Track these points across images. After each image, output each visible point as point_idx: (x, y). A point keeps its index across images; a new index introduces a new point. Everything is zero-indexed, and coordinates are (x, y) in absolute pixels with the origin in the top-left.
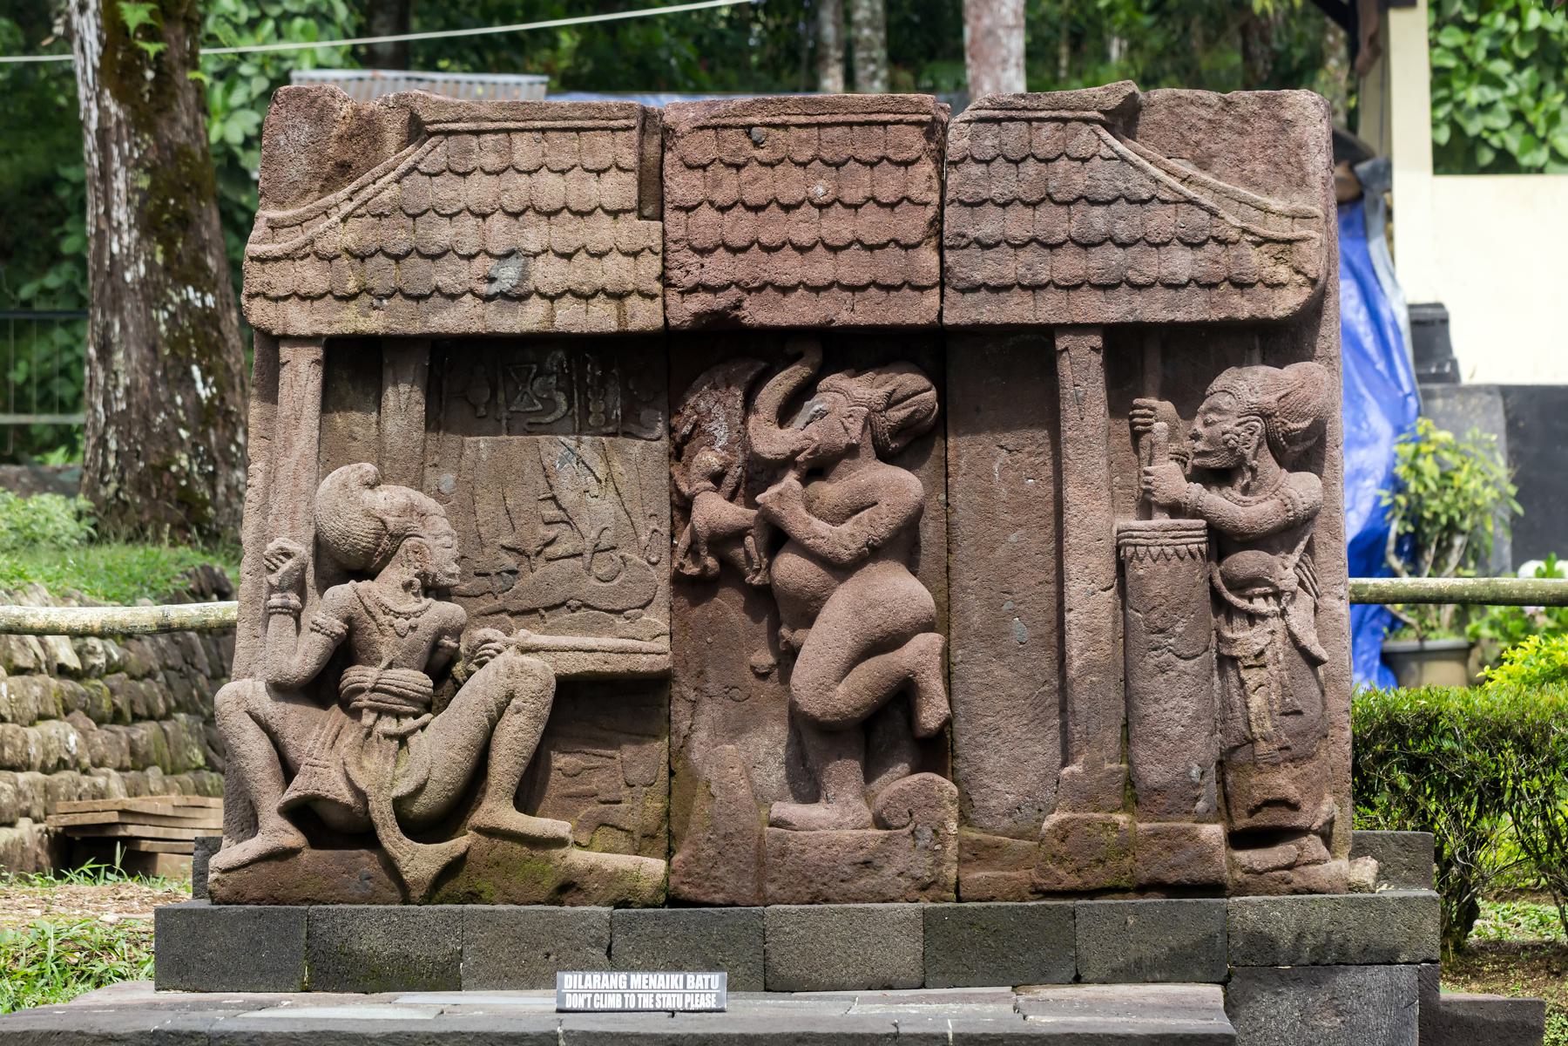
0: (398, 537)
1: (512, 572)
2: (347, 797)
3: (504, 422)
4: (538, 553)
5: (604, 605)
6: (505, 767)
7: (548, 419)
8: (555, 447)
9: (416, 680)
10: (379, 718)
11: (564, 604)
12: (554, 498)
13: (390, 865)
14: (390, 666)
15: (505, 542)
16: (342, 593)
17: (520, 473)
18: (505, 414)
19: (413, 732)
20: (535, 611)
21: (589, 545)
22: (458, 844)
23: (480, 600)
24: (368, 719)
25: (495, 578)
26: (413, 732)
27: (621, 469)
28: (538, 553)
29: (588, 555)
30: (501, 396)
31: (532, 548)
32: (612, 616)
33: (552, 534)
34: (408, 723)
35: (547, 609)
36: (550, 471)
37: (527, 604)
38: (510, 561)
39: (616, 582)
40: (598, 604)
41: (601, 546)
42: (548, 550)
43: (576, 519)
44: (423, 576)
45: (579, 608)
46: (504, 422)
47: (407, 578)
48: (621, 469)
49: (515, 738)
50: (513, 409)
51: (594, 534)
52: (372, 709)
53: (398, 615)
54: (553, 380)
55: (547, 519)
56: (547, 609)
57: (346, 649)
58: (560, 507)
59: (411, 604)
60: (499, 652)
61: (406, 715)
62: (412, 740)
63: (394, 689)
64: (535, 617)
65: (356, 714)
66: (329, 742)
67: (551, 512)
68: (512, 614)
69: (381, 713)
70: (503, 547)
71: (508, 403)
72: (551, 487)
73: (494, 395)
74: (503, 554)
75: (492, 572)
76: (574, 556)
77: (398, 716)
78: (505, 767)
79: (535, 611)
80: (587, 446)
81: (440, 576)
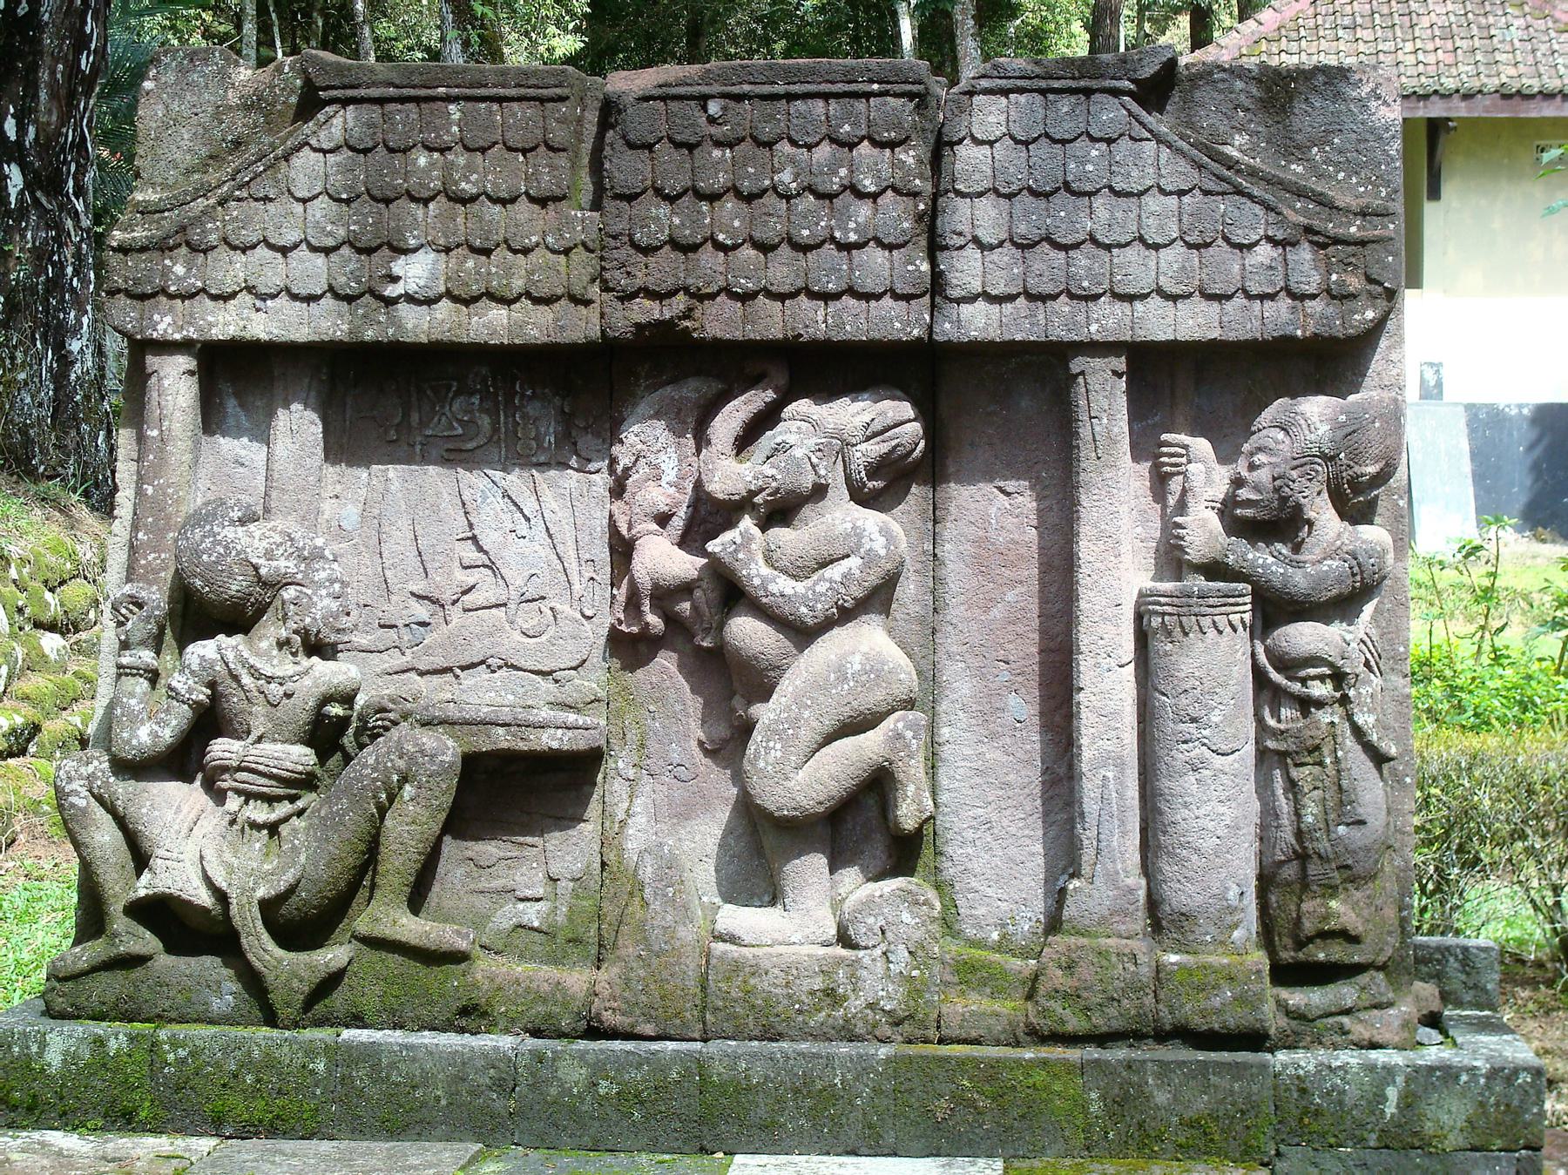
0: (274, 585)
1: (423, 624)
2: (204, 898)
3: (418, 448)
4: (454, 602)
5: (529, 665)
6: (398, 861)
7: (470, 446)
8: (475, 482)
9: (300, 756)
10: (246, 802)
11: (483, 662)
12: (474, 539)
13: (253, 981)
14: (259, 740)
15: (415, 589)
16: (204, 650)
17: (435, 509)
18: (419, 439)
19: (286, 819)
20: (448, 670)
21: (514, 595)
22: (333, 955)
23: (384, 656)
24: (233, 803)
25: (403, 631)
26: (286, 819)
27: (554, 506)
28: (454, 602)
29: (512, 606)
30: (415, 417)
31: (447, 597)
32: (538, 678)
33: (471, 581)
34: (284, 809)
35: (463, 668)
36: (469, 507)
37: (440, 662)
38: (422, 611)
39: (544, 638)
40: (522, 663)
41: (528, 596)
42: (465, 598)
43: (498, 564)
44: (304, 633)
45: (500, 667)
46: (418, 448)
47: (284, 633)
48: (554, 506)
49: (408, 828)
50: (430, 432)
51: (520, 582)
52: (238, 792)
53: (269, 680)
54: (476, 400)
55: (466, 562)
56: (463, 668)
57: (210, 720)
58: (480, 549)
59: (283, 666)
60: (395, 723)
61: (279, 799)
62: (284, 830)
63: (261, 768)
64: (449, 677)
65: (219, 797)
66: (185, 831)
67: (470, 553)
68: (422, 674)
69: (248, 796)
70: (413, 594)
71: (423, 424)
72: (471, 526)
73: (406, 415)
74: (413, 602)
75: (400, 623)
76: (497, 606)
77: (270, 800)
78: (398, 861)
79: (448, 670)
80: (515, 480)
81: (325, 631)
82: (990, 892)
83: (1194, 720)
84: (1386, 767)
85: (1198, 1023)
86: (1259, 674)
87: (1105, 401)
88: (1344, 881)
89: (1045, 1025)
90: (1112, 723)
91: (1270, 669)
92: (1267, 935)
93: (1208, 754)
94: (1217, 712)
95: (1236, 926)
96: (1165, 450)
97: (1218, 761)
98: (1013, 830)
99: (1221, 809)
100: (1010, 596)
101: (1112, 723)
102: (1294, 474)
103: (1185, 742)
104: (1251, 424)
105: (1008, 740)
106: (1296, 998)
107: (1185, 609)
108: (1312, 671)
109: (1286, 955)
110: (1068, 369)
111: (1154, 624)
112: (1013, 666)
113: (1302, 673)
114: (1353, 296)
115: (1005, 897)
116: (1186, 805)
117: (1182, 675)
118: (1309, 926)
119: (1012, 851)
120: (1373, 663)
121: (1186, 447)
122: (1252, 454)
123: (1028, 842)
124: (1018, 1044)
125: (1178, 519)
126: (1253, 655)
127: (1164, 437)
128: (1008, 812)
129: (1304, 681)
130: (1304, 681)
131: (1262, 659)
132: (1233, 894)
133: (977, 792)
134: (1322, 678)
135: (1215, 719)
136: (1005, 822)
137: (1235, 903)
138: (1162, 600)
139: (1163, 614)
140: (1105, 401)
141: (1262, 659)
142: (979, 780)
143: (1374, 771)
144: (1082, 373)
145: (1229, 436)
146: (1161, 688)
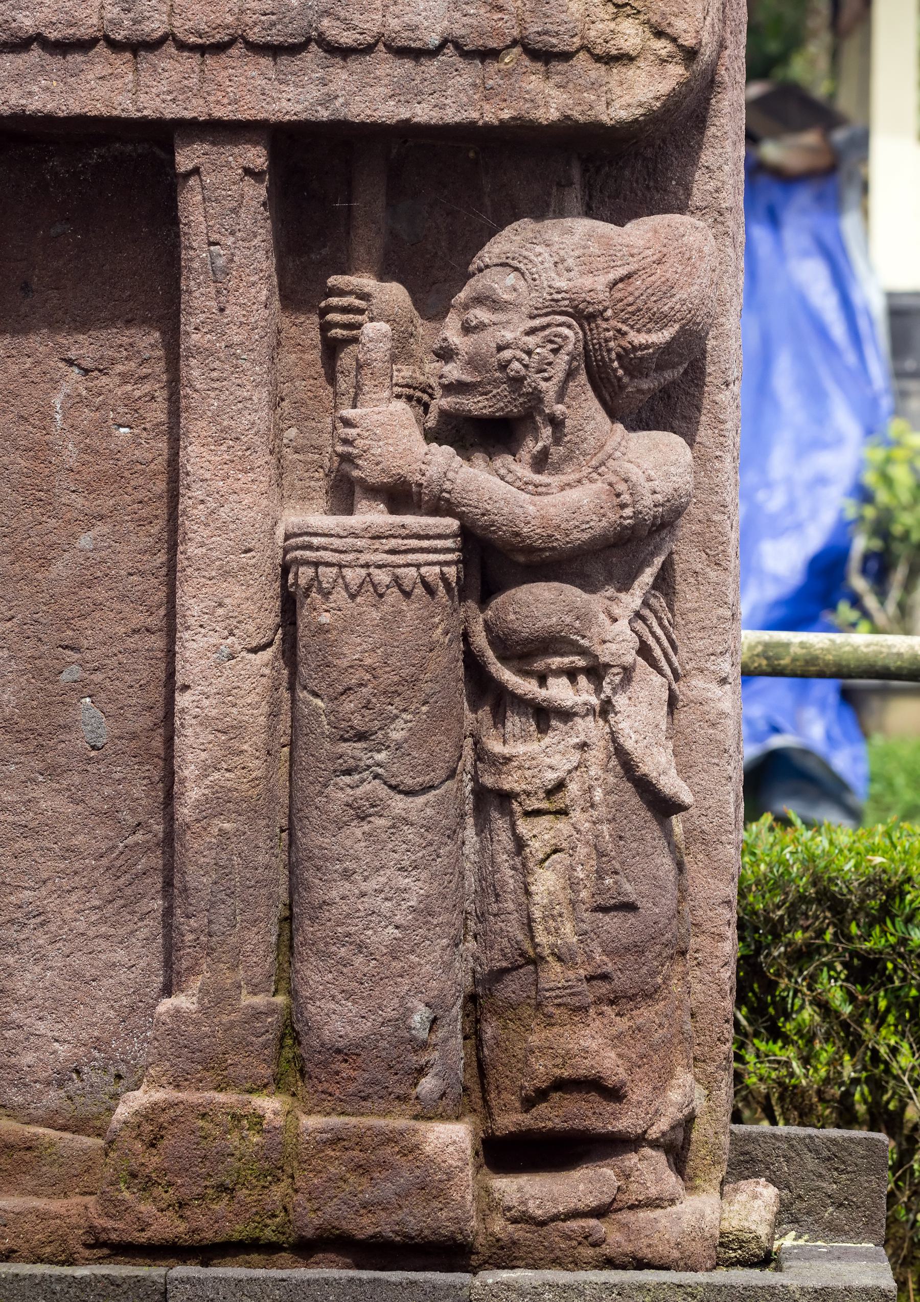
82: (42, 1027)
83: (361, 736)
84: (677, 823)
85: (365, 1226)
86: (474, 667)
87: (225, 218)
88: (599, 1001)
89: (119, 1229)
90: (235, 744)
91: (490, 654)
92: (477, 1087)
93: (383, 791)
94: (399, 723)
95: (421, 1071)
96: (334, 301)
97: (399, 804)
98: (81, 926)
99: (404, 882)
100: (85, 541)
101: (235, 744)
102: (531, 341)
103: (348, 772)
104: (469, 263)
105: (77, 779)
106: (512, 1188)
107: (350, 557)
108: (556, 662)
109: (510, 1121)
110: (172, 163)
111: (302, 581)
112: (88, 656)
113: (539, 665)
114: (625, 58)
115: (65, 1036)
116: (347, 875)
117: (345, 663)
118: (543, 1069)
119: (78, 961)
120: (658, 653)
121: (365, 297)
122: (466, 307)
123: (104, 944)
124: (70, 1262)
125: (348, 413)
126: (466, 637)
127: (334, 280)
128: (74, 897)
129: (542, 680)
130: (542, 680)
131: (481, 640)
132: (419, 1018)
133: (24, 864)
134: (572, 674)
135: (396, 736)
136: (69, 913)
137: (423, 1035)
138: (316, 541)
139: (316, 564)
140: (225, 218)
141: (481, 640)
142: (28, 845)
143: (654, 825)
144: (196, 171)
145: (435, 274)
146: (311, 684)
